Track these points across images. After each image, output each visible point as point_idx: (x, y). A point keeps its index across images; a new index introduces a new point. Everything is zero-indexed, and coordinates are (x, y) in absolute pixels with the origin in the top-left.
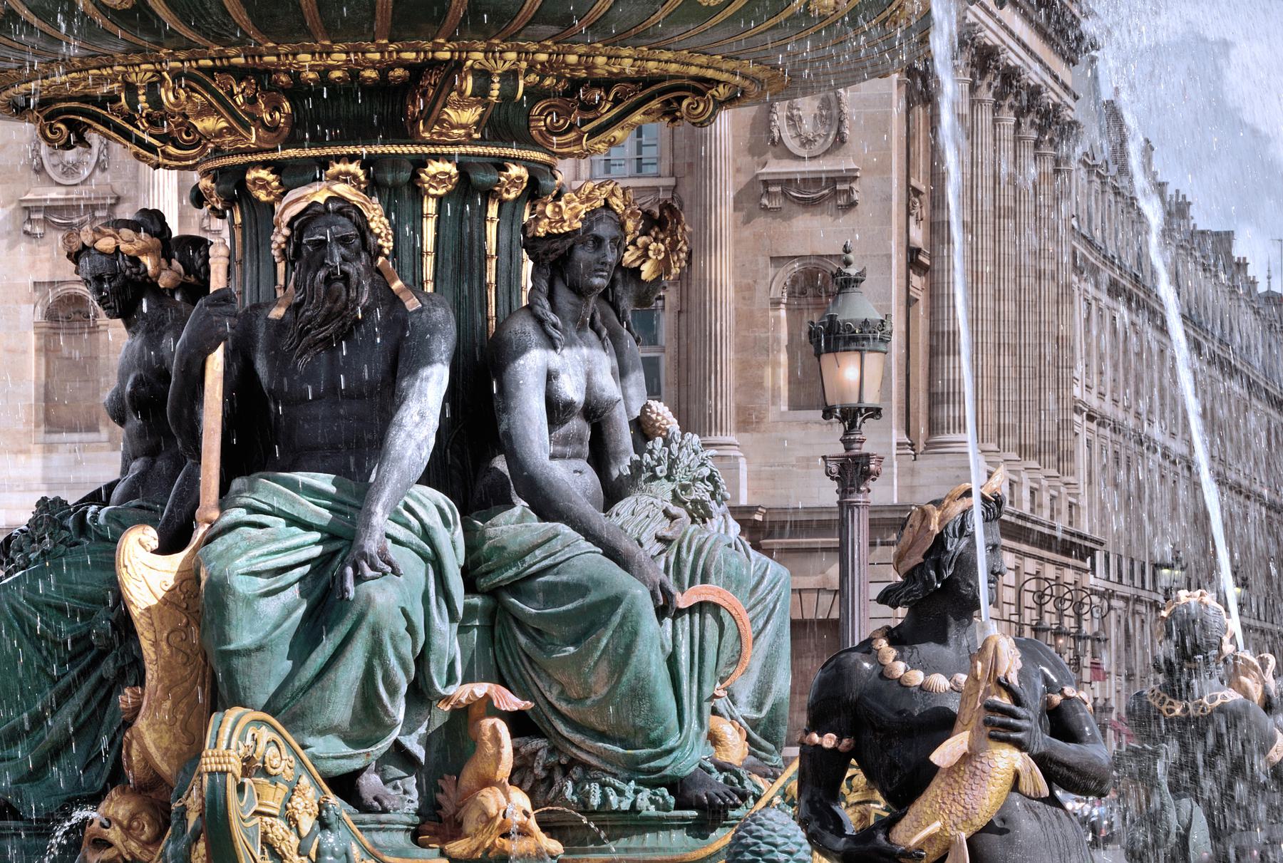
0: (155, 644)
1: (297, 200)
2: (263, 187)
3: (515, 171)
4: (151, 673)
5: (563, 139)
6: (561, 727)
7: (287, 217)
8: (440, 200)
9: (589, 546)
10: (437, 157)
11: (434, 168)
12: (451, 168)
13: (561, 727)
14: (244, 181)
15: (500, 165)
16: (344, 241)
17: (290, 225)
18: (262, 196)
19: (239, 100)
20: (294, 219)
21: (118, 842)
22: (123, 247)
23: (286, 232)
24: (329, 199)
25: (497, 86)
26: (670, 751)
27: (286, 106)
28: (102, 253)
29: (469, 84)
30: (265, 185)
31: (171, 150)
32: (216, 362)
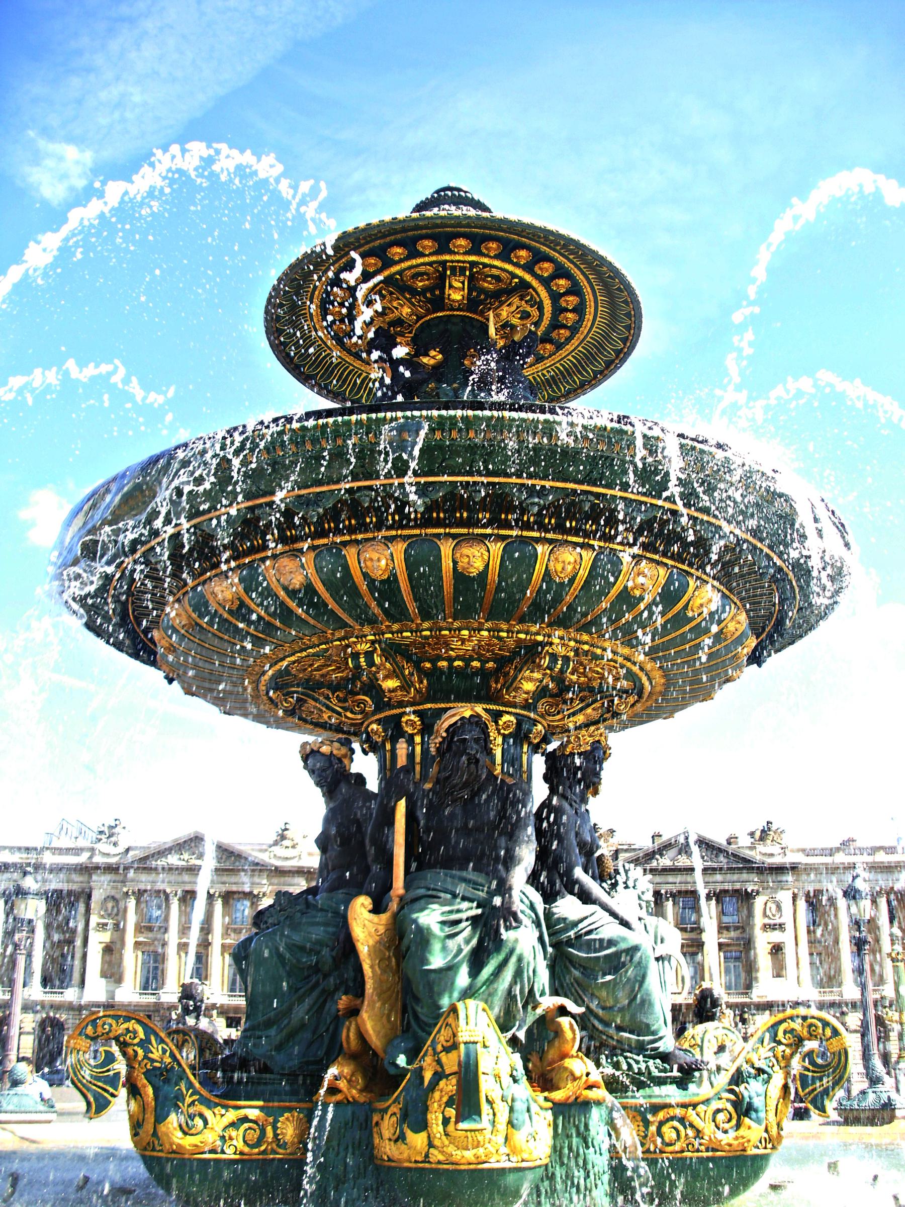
0: (372, 967)
1: (454, 715)
2: (412, 725)
3: (540, 727)
4: (369, 986)
5: (551, 718)
6: (596, 1023)
7: (446, 725)
8: (504, 736)
9: (611, 919)
10: (508, 713)
11: (506, 718)
12: (512, 718)
13: (596, 1023)
14: (401, 722)
15: (535, 722)
16: (477, 741)
17: (447, 731)
18: (409, 730)
19: (407, 672)
20: (451, 726)
21: (345, 1089)
22: (335, 752)
23: (444, 735)
24: (471, 716)
25: (560, 662)
26: (661, 1038)
27: (425, 681)
28: (323, 755)
29: (546, 662)
30: (413, 724)
31: (349, 714)
32: (402, 806)
